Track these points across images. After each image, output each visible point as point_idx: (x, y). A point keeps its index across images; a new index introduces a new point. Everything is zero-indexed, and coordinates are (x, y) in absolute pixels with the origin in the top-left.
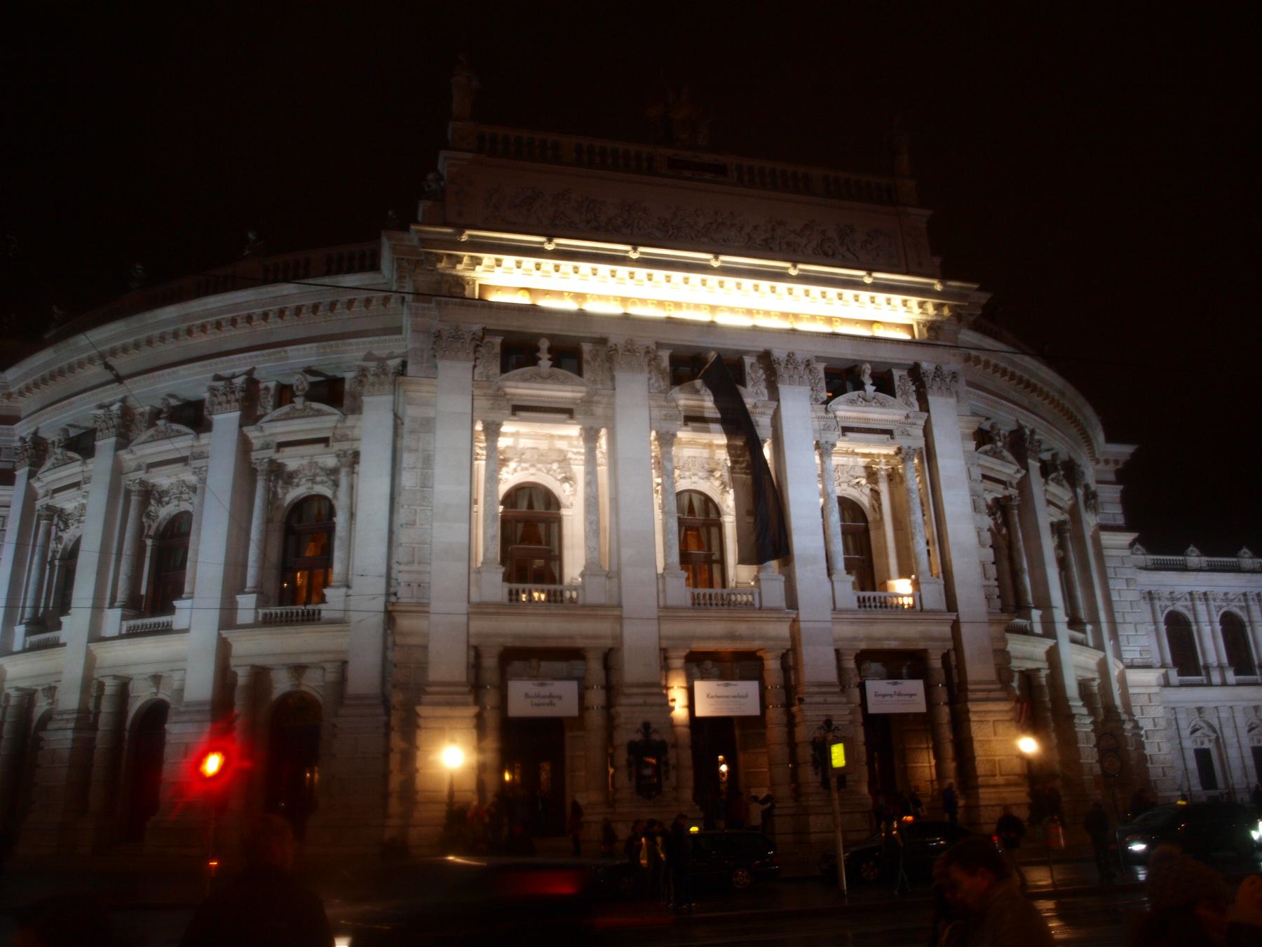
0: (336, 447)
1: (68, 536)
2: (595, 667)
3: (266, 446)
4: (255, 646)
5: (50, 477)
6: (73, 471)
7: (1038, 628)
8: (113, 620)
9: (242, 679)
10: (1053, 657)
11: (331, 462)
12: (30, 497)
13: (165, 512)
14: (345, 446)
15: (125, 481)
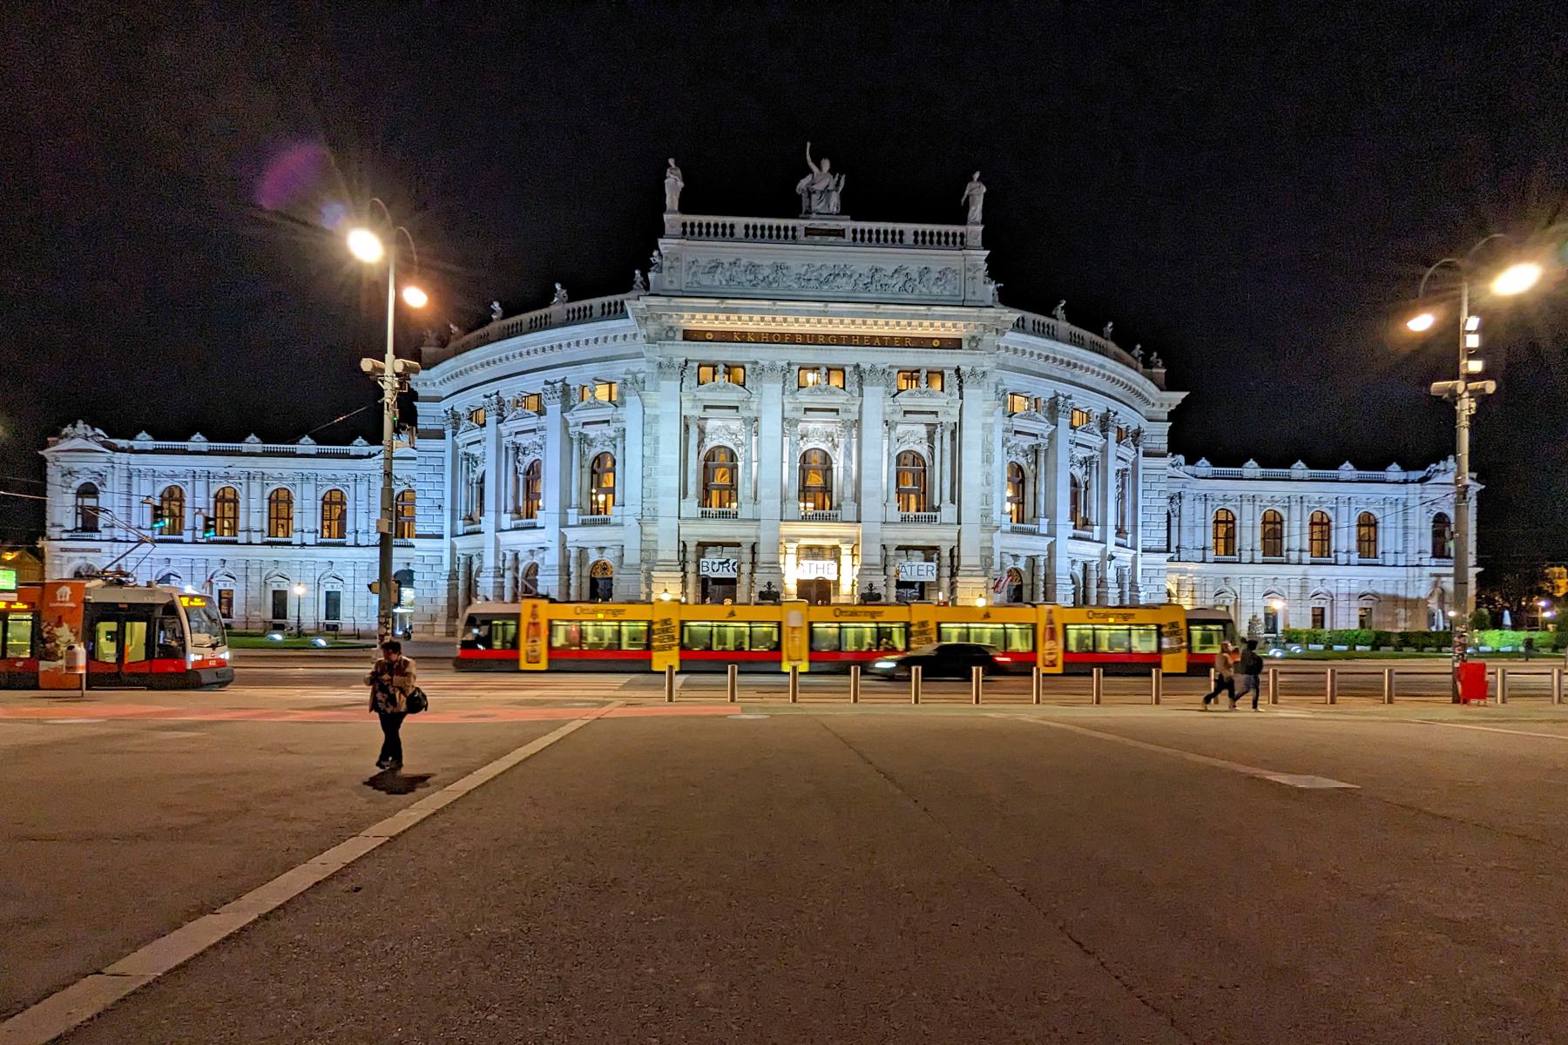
0: (613, 425)
1: (479, 470)
2: (746, 550)
3: (576, 425)
4: (576, 536)
5: (462, 438)
6: (476, 434)
7: (1044, 530)
8: (506, 520)
9: (574, 553)
10: (1051, 549)
11: (613, 434)
12: (455, 447)
13: (527, 461)
14: (618, 425)
15: (504, 441)
